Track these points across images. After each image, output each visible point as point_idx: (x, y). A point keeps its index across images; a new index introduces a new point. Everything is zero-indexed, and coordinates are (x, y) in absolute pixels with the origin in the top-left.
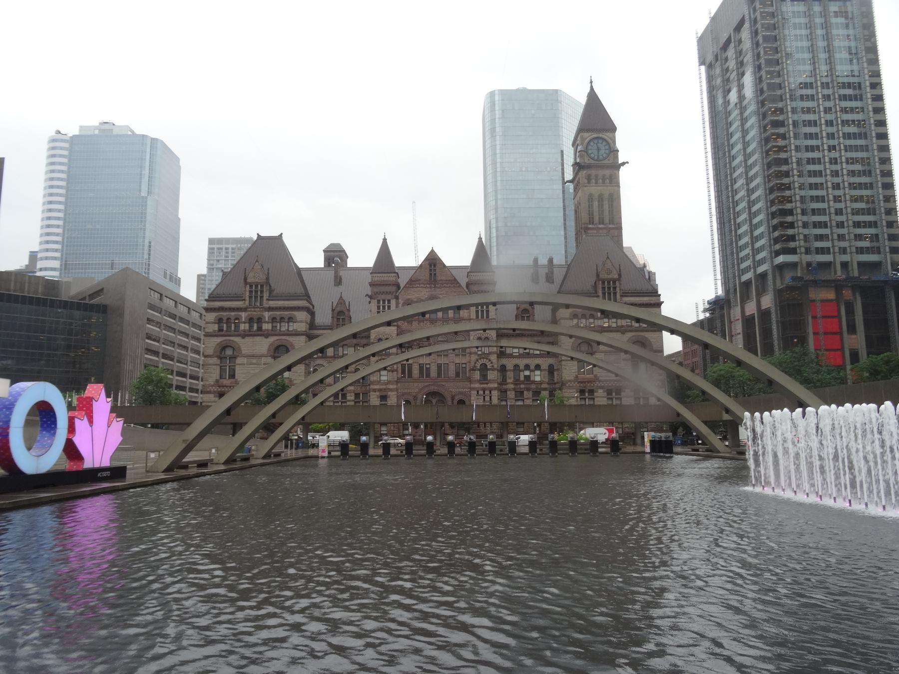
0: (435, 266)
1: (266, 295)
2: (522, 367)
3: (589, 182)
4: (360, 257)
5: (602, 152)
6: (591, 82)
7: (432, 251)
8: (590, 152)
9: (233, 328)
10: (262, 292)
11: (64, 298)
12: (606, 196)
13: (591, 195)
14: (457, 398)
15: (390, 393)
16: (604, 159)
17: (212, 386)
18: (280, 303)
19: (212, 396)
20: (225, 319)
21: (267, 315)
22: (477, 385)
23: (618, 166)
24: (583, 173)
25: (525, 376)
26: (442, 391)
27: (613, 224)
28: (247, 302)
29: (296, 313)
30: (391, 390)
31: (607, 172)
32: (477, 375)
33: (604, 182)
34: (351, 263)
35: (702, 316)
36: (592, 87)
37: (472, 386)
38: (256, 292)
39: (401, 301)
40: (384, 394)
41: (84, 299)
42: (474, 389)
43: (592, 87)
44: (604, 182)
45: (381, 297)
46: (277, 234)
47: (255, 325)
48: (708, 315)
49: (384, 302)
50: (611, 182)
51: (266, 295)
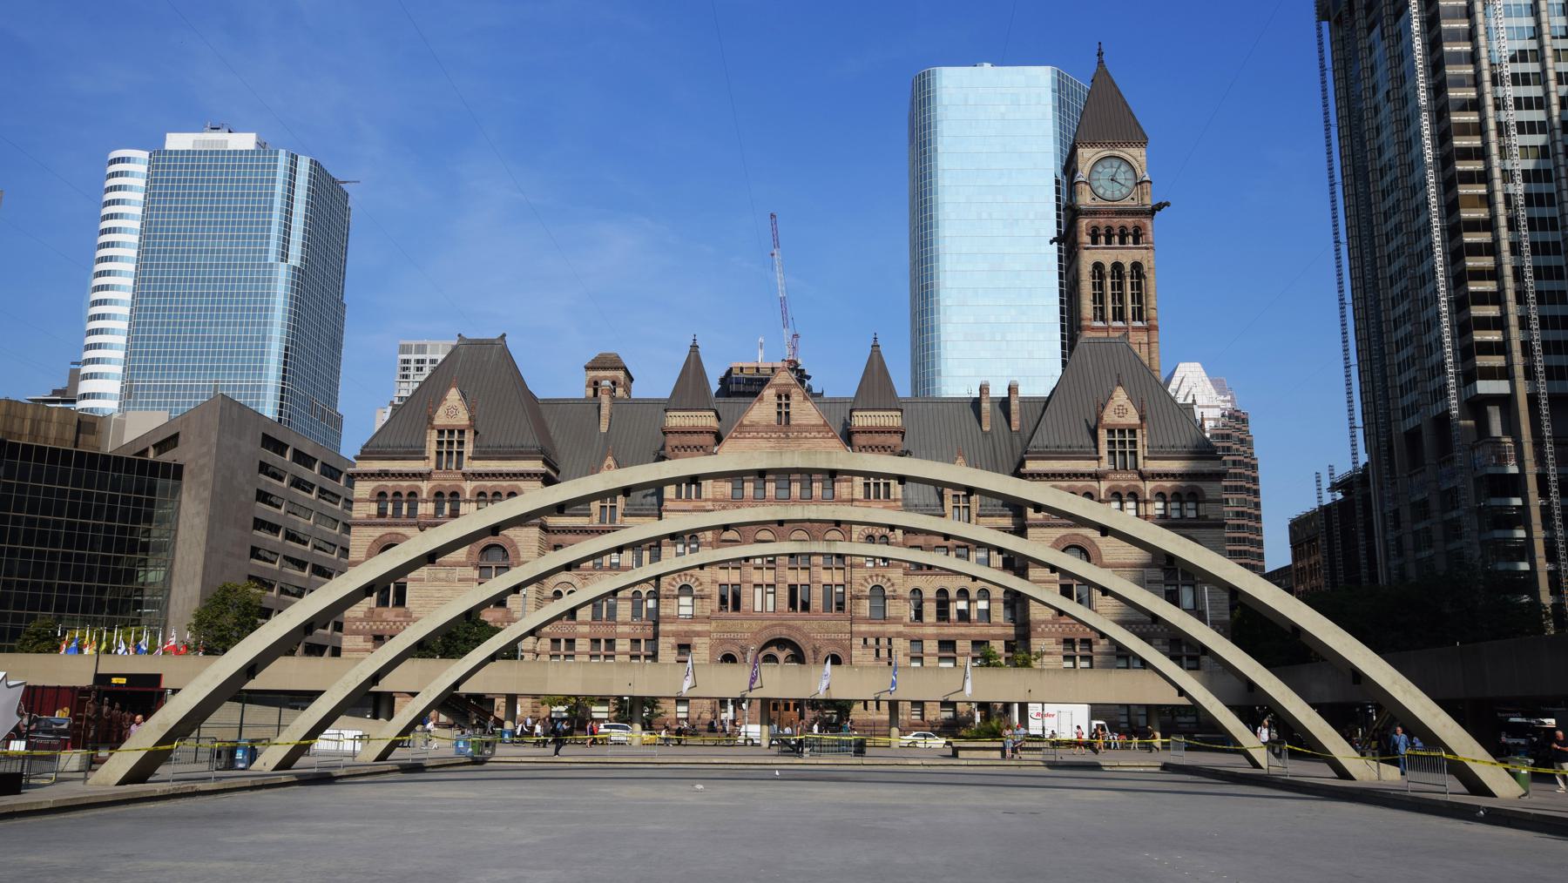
0: (788, 397)
1: (468, 449)
2: (953, 594)
6: (1100, 54)
8: (1095, 184)
9: (405, 511)
10: (461, 443)
11: (110, 447)
13: (1098, 266)
14: (825, 652)
15: (696, 640)
17: (361, 620)
19: (361, 638)
20: (390, 493)
21: (469, 487)
22: (864, 628)
25: (960, 612)
26: (796, 638)
27: (1141, 319)
28: (432, 465)
30: (698, 634)
31: (1129, 222)
32: (864, 608)
33: (1122, 241)
35: (1327, 499)
36: (1101, 62)
37: (855, 628)
38: (451, 443)
40: (684, 641)
41: (145, 452)
42: (860, 634)
43: (1101, 62)
44: (1122, 241)
46: (495, 335)
47: (447, 506)
48: (1339, 496)
50: (1136, 241)
51: (468, 449)
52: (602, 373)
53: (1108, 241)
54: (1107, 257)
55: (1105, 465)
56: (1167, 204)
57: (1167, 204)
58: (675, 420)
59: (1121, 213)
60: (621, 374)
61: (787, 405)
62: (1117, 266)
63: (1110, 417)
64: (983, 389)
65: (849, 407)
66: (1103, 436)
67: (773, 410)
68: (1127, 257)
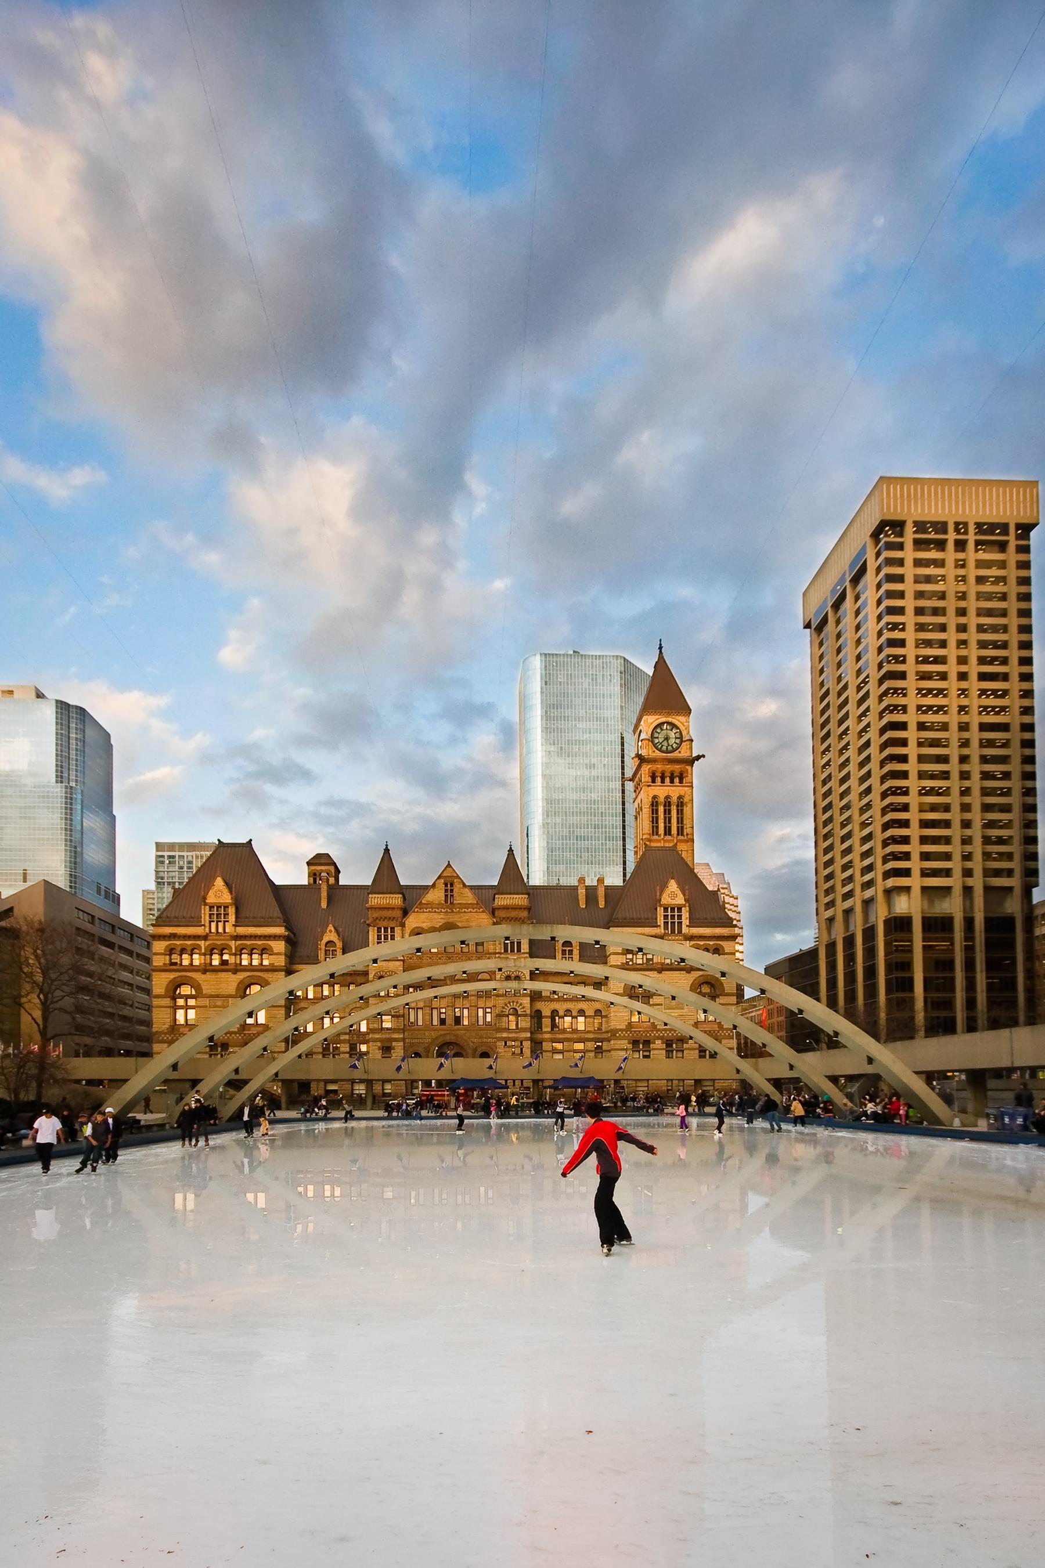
0: (452, 885)
3: (654, 781)
4: (356, 873)
5: (672, 741)
7: (449, 865)
12: (674, 799)
13: (655, 797)
16: (674, 750)
18: (251, 930)
23: (691, 761)
24: (646, 769)
29: (272, 943)
31: (677, 768)
33: (672, 782)
34: (343, 881)
39: (408, 930)
45: (383, 924)
49: (386, 929)
50: (681, 782)
52: (319, 868)
53: (663, 782)
54: (661, 791)
55: (661, 931)
56: (703, 756)
57: (703, 756)
58: (375, 900)
59: (672, 761)
60: (332, 869)
61: (452, 891)
62: (667, 797)
63: (666, 899)
64: (582, 880)
65: (491, 892)
66: (660, 911)
67: (442, 894)
68: (674, 791)
